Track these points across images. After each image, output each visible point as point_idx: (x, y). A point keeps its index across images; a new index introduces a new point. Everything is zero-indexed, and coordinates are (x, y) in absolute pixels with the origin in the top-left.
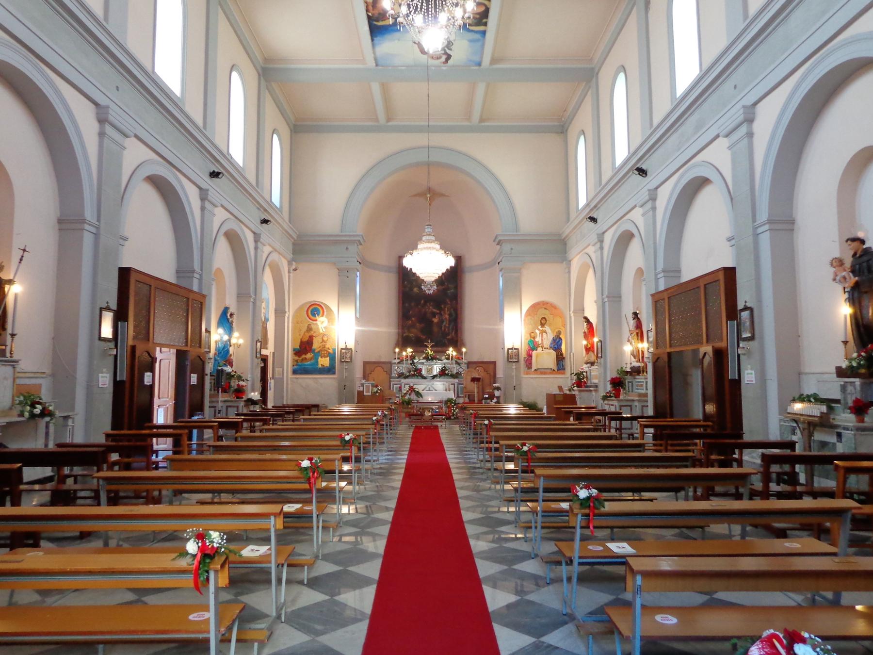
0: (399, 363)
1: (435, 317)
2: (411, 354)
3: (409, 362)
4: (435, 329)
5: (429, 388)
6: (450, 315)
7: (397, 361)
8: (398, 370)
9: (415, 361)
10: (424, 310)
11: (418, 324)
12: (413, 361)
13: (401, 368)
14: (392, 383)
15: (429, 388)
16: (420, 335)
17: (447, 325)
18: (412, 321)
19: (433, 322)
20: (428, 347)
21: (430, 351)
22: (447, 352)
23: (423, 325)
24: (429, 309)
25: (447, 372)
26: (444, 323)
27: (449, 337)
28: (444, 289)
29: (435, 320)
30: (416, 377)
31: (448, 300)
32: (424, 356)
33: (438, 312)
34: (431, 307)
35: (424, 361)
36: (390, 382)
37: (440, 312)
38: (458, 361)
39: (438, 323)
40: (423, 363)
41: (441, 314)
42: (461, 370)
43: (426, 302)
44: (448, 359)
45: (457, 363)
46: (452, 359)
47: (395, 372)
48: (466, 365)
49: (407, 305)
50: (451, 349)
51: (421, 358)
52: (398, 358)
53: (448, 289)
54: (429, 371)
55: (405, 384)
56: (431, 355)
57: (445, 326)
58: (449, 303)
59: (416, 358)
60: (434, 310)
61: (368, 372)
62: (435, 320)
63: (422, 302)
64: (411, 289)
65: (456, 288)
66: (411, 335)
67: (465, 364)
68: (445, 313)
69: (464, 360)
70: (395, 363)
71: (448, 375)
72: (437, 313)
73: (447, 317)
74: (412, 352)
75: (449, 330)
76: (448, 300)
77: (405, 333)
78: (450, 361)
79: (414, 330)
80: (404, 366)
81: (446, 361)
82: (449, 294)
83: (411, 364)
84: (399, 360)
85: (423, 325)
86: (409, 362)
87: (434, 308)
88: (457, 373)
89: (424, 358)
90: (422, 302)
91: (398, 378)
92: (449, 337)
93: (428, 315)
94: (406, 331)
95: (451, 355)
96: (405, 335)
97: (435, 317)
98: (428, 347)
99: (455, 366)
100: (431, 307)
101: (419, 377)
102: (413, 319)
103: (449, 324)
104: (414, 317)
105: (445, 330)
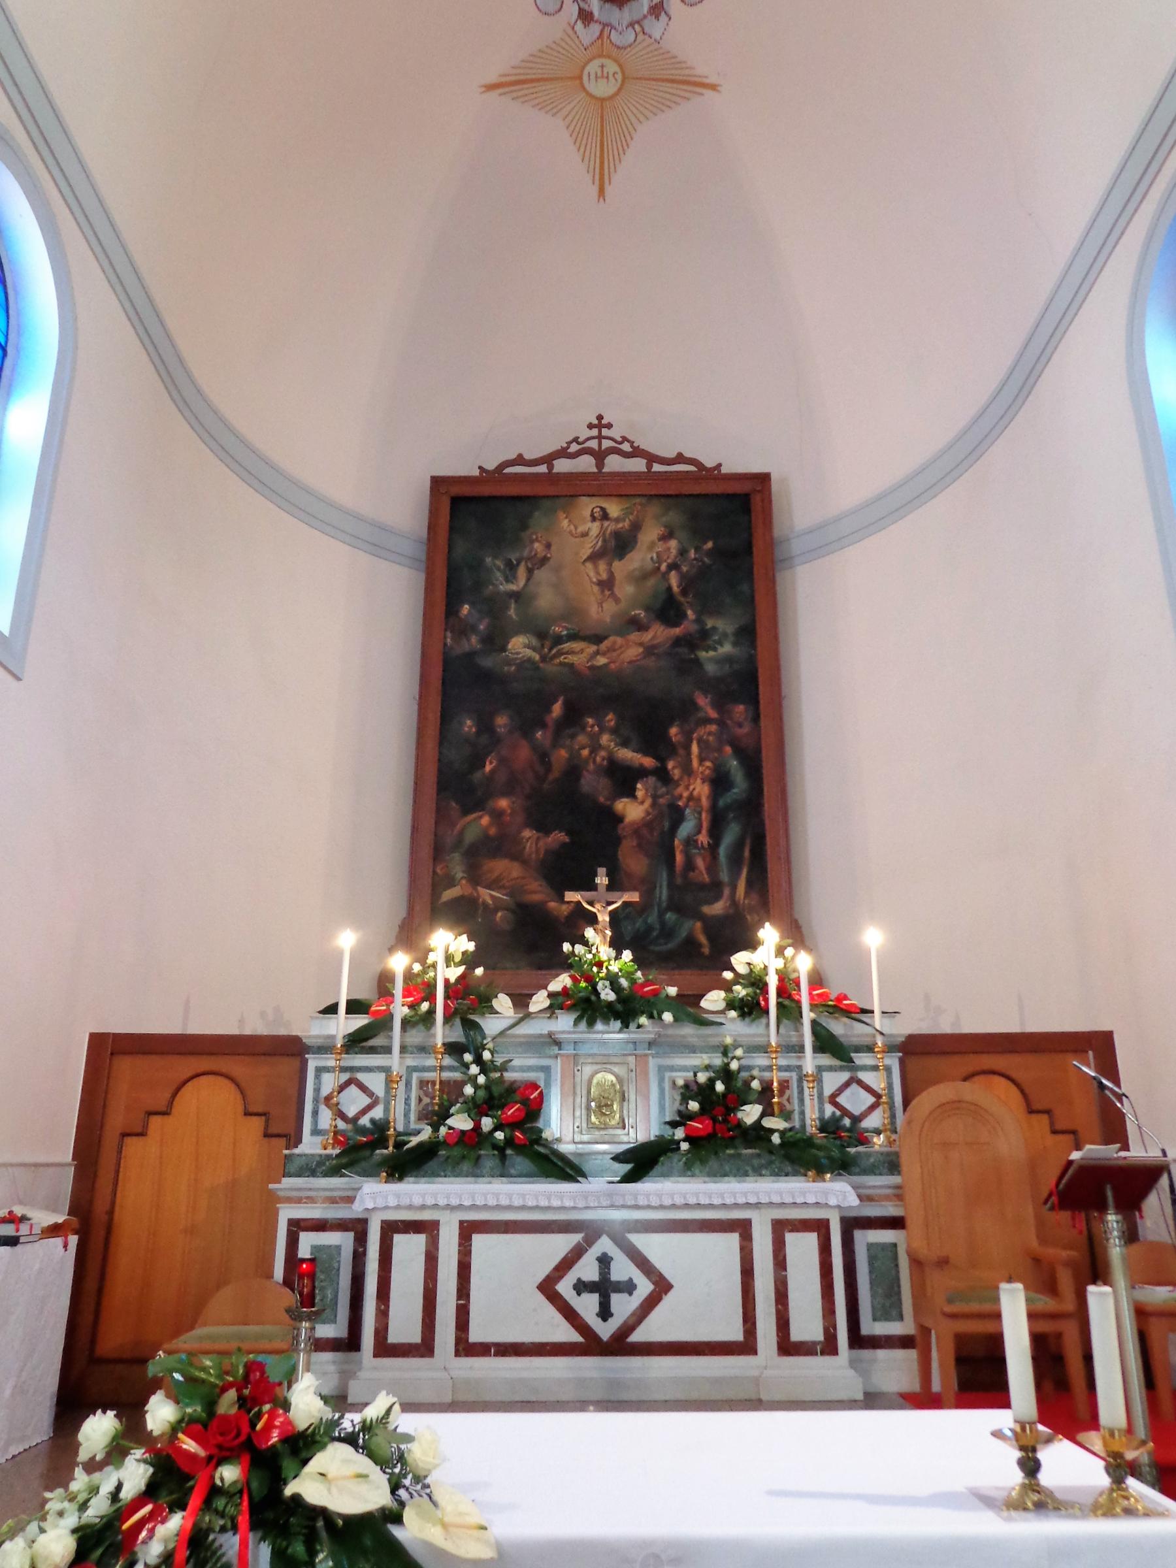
0: (356, 1042)
1: (631, 793)
2: (454, 973)
3: (440, 1034)
4: (634, 862)
5: (604, 1261)
6: (720, 782)
7: (344, 1025)
8: (353, 1101)
9: (491, 1026)
10: (563, 753)
11: (527, 833)
12: (470, 1026)
13: (376, 1083)
14: (286, 1214)
15: (604, 1261)
16: (537, 892)
17: (703, 839)
18: (497, 815)
19: (619, 819)
20: (592, 920)
21: (605, 952)
22: (740, 960)
23: (559, 837)
24: (595, 748)
25: (750, 1114)
26: (685, 829)
27: (717, 908)
28: (678, 642)
29: (633, 810)
30: (489, 1160)
31: (703, 702)
32: (562, 981)
33: (648, 762)
34: (605, 739)
35: (564, 1023)
36: (271, 1203)
37: (662, 760)
38: (838, 1027)
39: (647, 824)
40: (554, 1041)
41: (662, 775)
42: (855, 1101)
43: (573, 718)
44: (751, 1009)
45: (826, 1043)
46: (789, 1009)
47: (326, 1118)
48: (893, 1061)
49: (469, 725)
50: (769, 934)
51: (540, 1001)
52: (354, 1007)
53: (702, 638)
54: (603, 1106)
55: (390, 1229)
56: (613, 980)
57: (690, 842)
58: (713, 714)
59: (503, 1003)
60: (627, 755)
61: (117, 1119)
62: (633, 810)
63: (557, 709)
64: (495, 641)
65: (747, 634)
66: (486, 895)
67: (890, 1049)
68: (688, 771)
69: (877, 1020)
70: (325, 1049)
71: (758, 1134)
72: (641, 773)
73: (701, 789)
74: (470, 960)
75: (712, 867)
76: (703, 702)
77: (451, 882)
78: (770, 1030)
79: (500, 866)
80: (395, 1061)
81: (734, 1028)
82: (711, 668)
83: (454, 1049)
84: (360, 1021)
85: (559, 837)
86: (440, 1034)
87: (625, 744)
88: (829, 1127)
89: (559, 1002)
90: (557, 709)
91: (335, 1171)
92: (717, 908)
93: (593, 784)
94: (459, 872)
95: (773, 982)
96: (448, 895)
97: (631, 793)
98: (592, 920)
99: (810, 1061)
100: (605, 739)
101: (520, 1163)
102: (503, 803)
103: (716, 832)
104: (505, 793)
105: (690, 865)
